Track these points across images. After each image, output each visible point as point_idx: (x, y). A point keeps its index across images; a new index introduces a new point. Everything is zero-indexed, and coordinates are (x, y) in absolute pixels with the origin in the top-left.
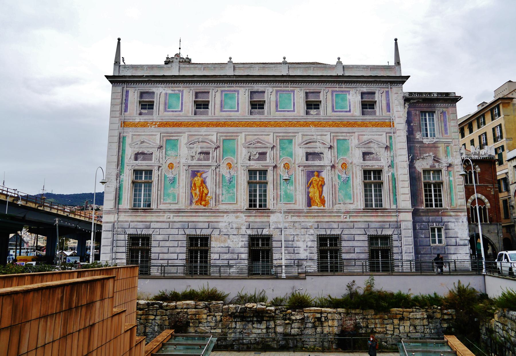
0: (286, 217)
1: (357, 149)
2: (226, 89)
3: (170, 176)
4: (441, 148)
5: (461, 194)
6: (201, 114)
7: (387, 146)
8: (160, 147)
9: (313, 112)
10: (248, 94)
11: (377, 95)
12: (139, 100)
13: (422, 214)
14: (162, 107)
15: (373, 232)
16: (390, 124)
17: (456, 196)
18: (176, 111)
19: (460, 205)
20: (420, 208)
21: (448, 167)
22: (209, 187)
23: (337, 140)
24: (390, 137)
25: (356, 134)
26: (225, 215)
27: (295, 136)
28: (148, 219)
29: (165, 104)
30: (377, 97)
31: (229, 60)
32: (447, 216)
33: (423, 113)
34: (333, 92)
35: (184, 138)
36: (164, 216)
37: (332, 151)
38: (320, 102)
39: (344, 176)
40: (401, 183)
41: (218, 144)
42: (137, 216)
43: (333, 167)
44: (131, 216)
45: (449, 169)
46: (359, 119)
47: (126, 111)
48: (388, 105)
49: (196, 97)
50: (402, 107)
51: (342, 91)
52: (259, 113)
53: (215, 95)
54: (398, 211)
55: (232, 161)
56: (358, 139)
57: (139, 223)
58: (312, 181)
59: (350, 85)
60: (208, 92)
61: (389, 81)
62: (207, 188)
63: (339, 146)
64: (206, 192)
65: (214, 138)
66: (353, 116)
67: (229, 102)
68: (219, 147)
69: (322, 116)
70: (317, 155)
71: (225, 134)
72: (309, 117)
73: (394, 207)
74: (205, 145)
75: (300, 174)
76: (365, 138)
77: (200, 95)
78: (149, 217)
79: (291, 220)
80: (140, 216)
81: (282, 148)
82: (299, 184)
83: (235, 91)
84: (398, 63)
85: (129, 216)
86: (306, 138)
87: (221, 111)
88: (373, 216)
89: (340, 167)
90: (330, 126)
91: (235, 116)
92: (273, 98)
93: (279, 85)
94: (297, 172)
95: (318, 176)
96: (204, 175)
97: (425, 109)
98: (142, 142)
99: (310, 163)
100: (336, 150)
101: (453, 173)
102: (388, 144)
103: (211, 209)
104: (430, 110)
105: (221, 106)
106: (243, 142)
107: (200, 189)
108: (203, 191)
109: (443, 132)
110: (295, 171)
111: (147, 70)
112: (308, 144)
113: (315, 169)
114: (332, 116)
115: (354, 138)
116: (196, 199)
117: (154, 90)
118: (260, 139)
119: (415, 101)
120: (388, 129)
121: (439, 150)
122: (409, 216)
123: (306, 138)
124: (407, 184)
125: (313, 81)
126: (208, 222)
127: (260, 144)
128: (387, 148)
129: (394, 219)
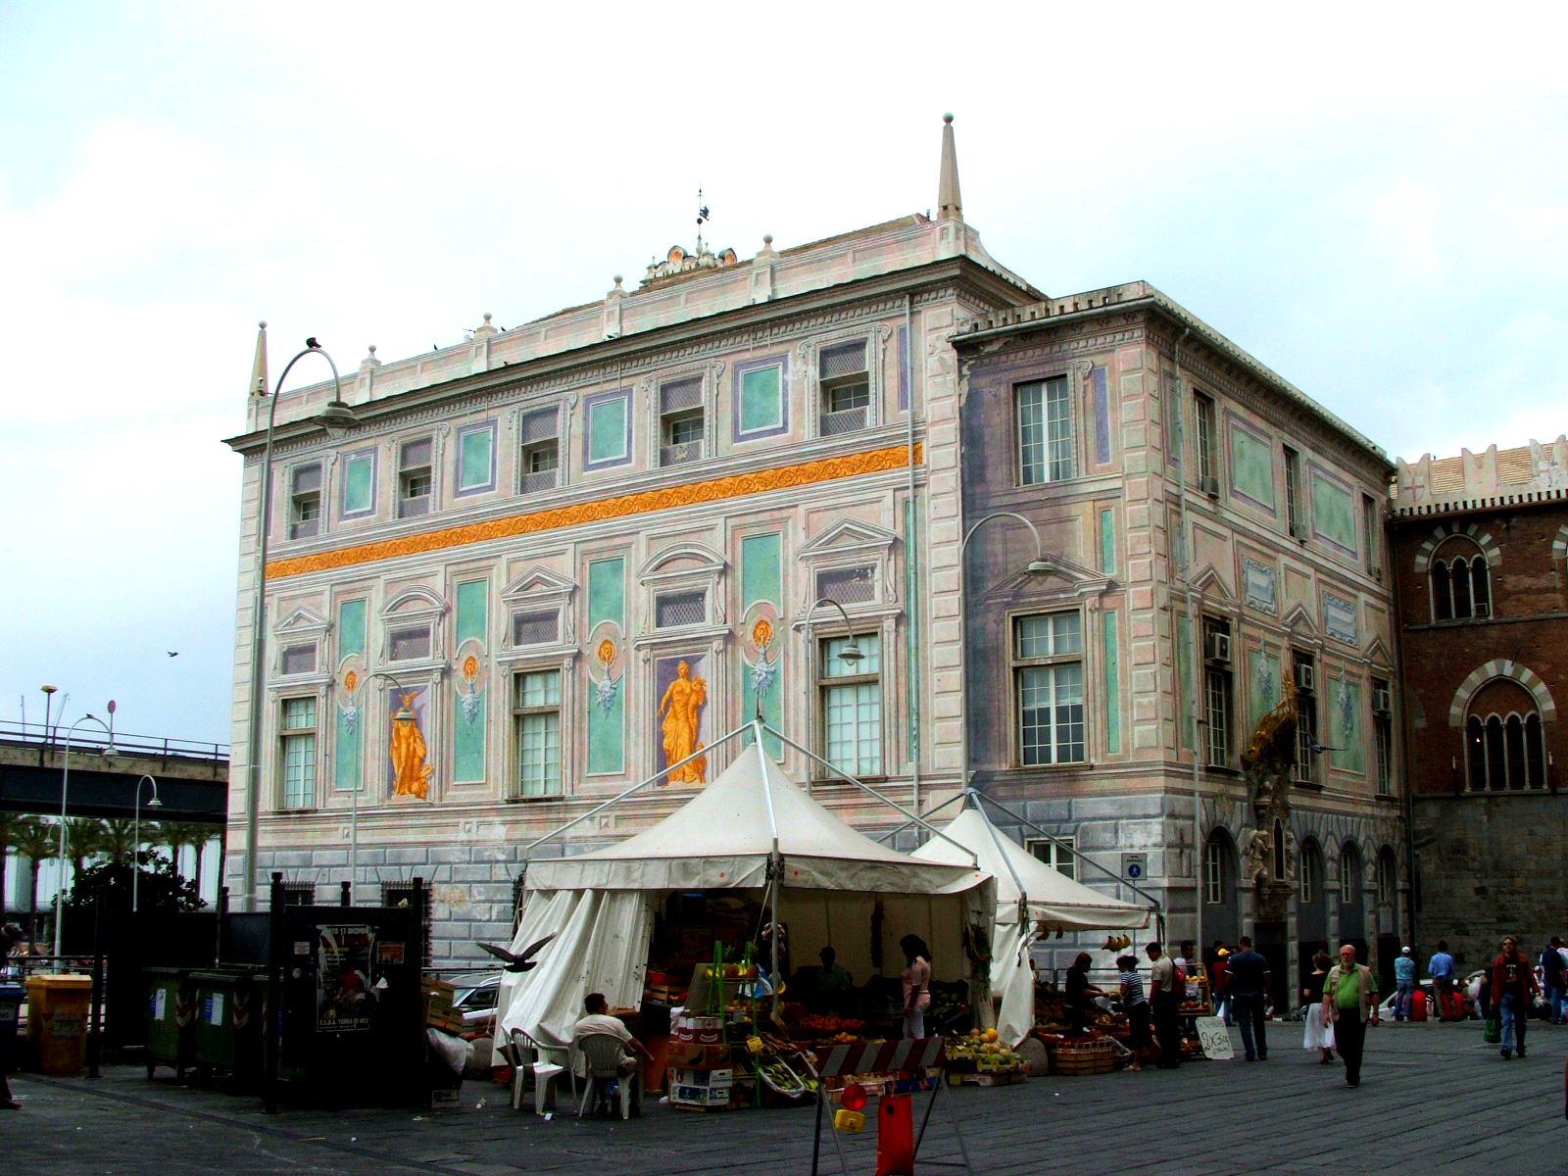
0: (604, 821)
1: (801, 565)
2: (466, 420)
3: (351, 710)
4: (1079, 524)
5: (1145, 700)
7: (896, 540)
8: (330, 628)
12: (291, 494)
13: (1001, 792)
17: (1125, 710)
18: (361, 514)
19: (1141, 749)
20: (995, 767)
21: (1102, 594)
22: (427, 737)
23: (745, 539)
25: (801, 509)
26: (462, 821)
27: (629, 546)
28: (309, 839)
29: (342, 498)
31: (482, 322)
32: (1090, 795)
34: (737, 366)
35: (377, 591)
36: (337, 829)
37: (729, 580)
38: (701, 410)
39: (761, 667)
40: (937, 675)
41: (447, 600)
42: (284, 831)
43: (730, 638)
44: (275, 831)
45: (1108, 602)
46: (811, 453)
49: (404, 460)
50: (953, 376)
51: (764, 361)
53: (444, 444)
55: (478, 648)
56: (807, 528)
57: (290, 853)
58: (671, 696)
59: (783, 333)
61: (906, 290)
62: (422, 739)
64: (420, 753)
65: (438, 583)
66: (793, 446)
67: (472, 460)
68: (448, 609)
69: (707, 463)
71: (463, 567)
72: (671, 472)
75: (641, 672)
76: (827, 522)
78: (311, 835)
79: (615, 833)
80: (294, 831)
81: (595, 593)
82: (637, 708)
83: (487, 423)
84: (951, 207)
85: (275, 831)
86: (660, 547)
88: (841, 807)
89: (750, 636)
94: (633, 669)
95: (688, 676)
98: (299, 618)
100: (739, 573)
101: (1122, 616)
102: (899, 532)
103: (432, 805)
104: (1048, 370)
105: (457, 481)
106: (504, 585)
107: (409, 745)
108: (415, 749)
109: (1092, 453)
110: (628, 664)
111: (307, 402)
112: (662, 570)
113: (680, 651)
114: (731, 458)
115: (795, 527)
116: (398, 772)
118: (541, 570)
119: (995, 347)
121: (1073, 532)
123: (660, 547)
124: (955, 678)
125: (673, 344)
126: (426, 843)
128: (896, 545)
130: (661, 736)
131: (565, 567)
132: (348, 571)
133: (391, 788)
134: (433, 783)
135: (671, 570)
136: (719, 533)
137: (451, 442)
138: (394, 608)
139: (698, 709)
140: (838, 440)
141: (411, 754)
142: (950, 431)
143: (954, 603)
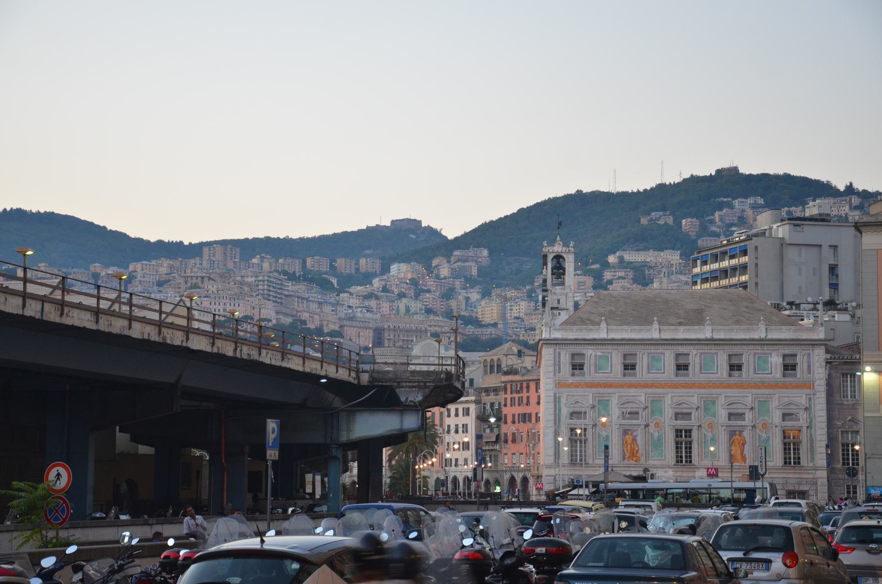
3: (604, 434)
6: (630, 375)
8: (593, 407)
9: (736, 373)
10: (673, 356)
11: (798, 357)
14: (593, 369)
15: (791, 488)
16: (808, 385)
22: (639, 444)
24: (810, 399)
29: (596, 366)
30: (799, 360)
33: (845, 375)
34: (755, 354)
39: (764, 435)
43: (754, 427)
47: (559, 372)
48: (809, 367)
49: (625, 359)
52: (685, 375)
54: (816, 469)
60: (636, 355)
63: (761, 406)
64: (636, 448)
65: (643, 399)
70: (741, 416)
72: (732, 379)
73: (811, 465)
74: (634, 405)
77: (628, 357)
81: (706, 409)
87: (649, 373)
90: (752, 388)
91: (661, 377)
92: (697, 360)
93: (703, 347)
95: (740, 435)
96: (635, 434)
97: (844, 371)
98: (577, 402)
99: (732, 423)
104: (851, 372)
105: (648, 369)
113: (737, 429)
116: (627, 455)
117: (584, 351)
120: (808, 391)
122: (824, 474)
127: (685, 406)
128: (806, 409)
129: (811, 476)
130: (731, 451)
131: (695, 401)
132: (601, 390)
133: (624, 458)
134: (643, 459)
135: (734, 406)
136: (750, 398)
137: (645, 357)
138: (623, 404)
139: (743, 444)
140: (788, 379)
141: (632, 450)
142: (823, 382)
143: (824, 425)
